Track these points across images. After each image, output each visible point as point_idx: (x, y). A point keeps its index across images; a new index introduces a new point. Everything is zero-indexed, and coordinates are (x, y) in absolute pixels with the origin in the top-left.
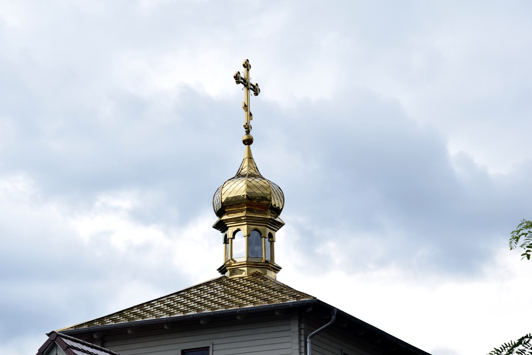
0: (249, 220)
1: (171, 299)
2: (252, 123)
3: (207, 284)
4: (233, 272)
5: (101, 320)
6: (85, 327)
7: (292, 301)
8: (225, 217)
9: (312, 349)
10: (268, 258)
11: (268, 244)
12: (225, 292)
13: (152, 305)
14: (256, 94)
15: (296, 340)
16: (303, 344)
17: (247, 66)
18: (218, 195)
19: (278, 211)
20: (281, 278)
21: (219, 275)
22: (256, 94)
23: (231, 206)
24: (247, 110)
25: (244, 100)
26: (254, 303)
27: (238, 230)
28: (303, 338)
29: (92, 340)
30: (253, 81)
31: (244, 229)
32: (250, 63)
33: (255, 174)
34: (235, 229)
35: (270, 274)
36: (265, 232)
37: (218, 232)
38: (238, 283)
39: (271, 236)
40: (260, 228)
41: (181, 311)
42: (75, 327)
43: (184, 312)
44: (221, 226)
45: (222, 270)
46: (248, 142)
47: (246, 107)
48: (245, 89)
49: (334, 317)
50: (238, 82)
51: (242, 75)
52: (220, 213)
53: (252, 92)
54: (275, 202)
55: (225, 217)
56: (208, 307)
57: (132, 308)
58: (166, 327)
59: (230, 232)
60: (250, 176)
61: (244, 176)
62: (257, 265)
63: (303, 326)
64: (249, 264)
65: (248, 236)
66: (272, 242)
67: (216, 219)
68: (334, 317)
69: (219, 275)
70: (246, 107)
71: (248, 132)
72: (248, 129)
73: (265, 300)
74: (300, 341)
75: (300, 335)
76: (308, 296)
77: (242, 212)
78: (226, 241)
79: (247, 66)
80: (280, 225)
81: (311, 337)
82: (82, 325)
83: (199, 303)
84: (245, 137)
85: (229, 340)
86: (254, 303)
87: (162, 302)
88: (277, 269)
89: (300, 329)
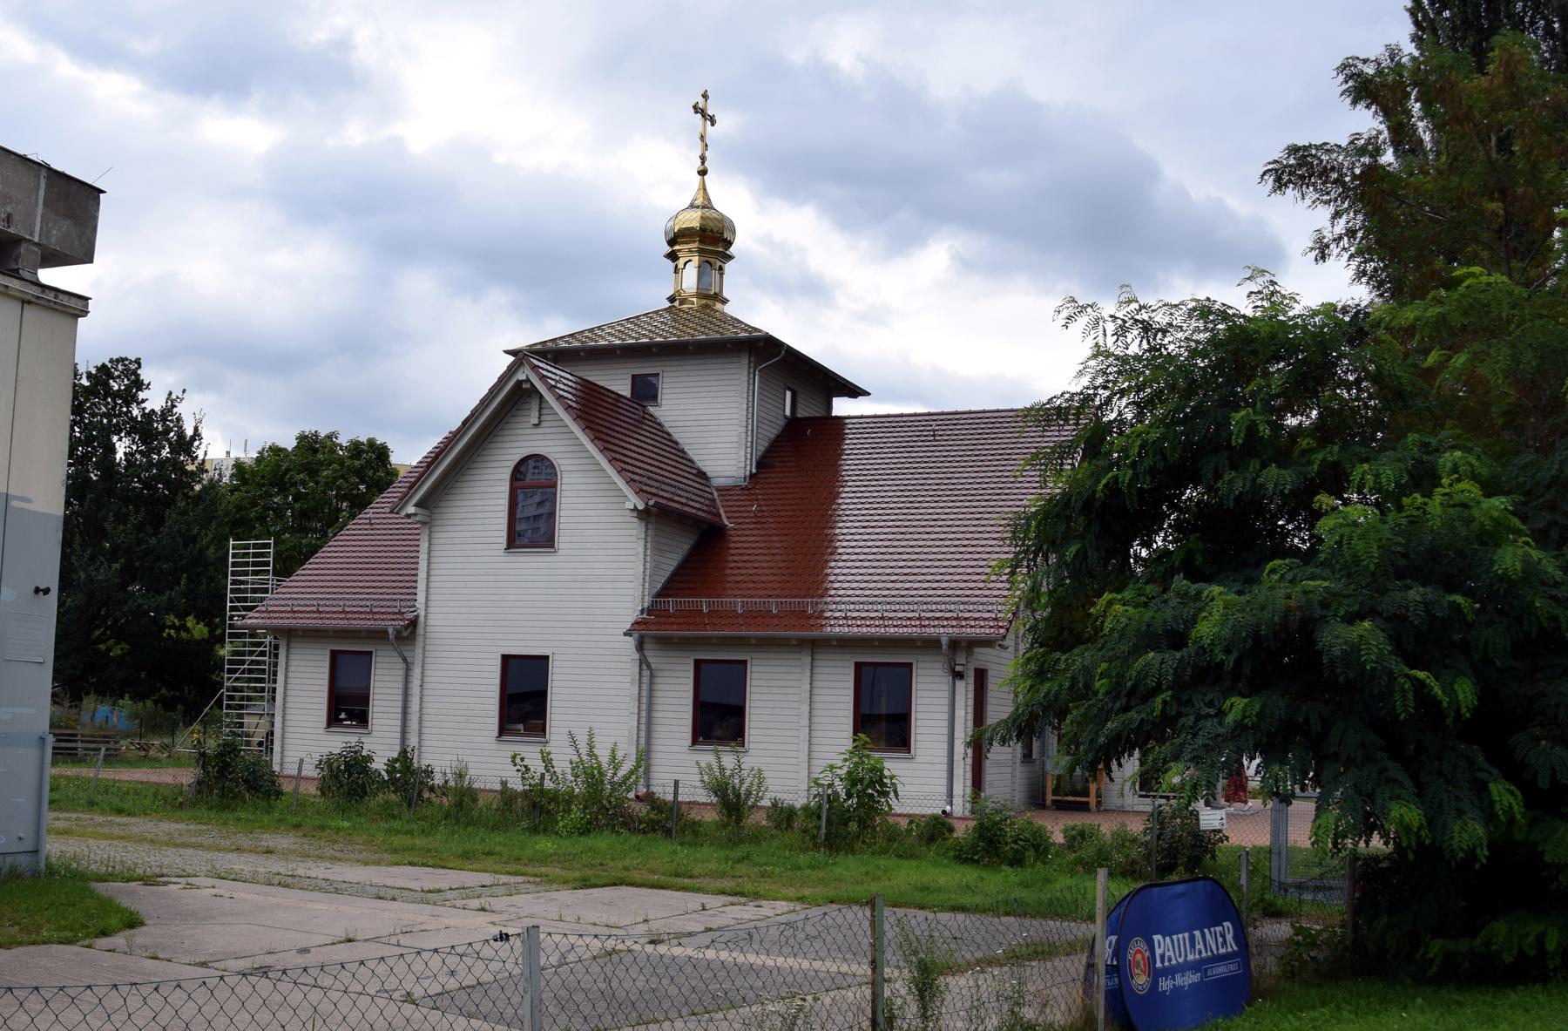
0: (701, 252)
1: (622, 325)
2: (707, 154)
3: (656, 312)
4: (681, 304)
5: (554, 340)
6: (539, 347)
7: (744, 334)
8: (677, 247)
9: (760, 382)
10: (717, 291)
11: (718, 275)
12: (675, 320)
13: (603, 330)
14: (713, 125)
15: (746, 372)
16: (752, 376)
17: (705, 96)
18: (671, 223)
19: (729, 244)
20: (729, 309)
21: (668, 304)
22: (713, 125)
23: (683, 236)
24: (702, 141)
25: (700, 129)
26: (707, 334)
27: (690, 261)
28: (752, 371)
29: (545, 358)
30: (710, 112)
31: (696, 260)
32: (709, 93)
33: (707, 205)
34: (687, 259)
35: (718, 306)
36: (715, 264)
37: (669, 262)
38: (687, 313)
39: (721, 268)
40: (712, 260)
41: (633, 338)
42: (530, 346)
43: (637, 339)
44: (673, 256)
45: (672, 299)
46: (703, 173)
47: (702, 138)
48: (702, 120)
49: (783, 352)
50: (696, 112)
51: (700, 106)
52: (671, 242)
53: (709, 123)
54: (726, 235)
55: (677, 247)
56: (661, 336)
57: (583, 332)
58: (618, 352)
59: (681, 263)
60: (704, 207)
61: (698, 207)
62: (707, 297)
63: (752, 359)
64: (700, 295)
65: (699, 267)
66: (722, 275)
67: (668, 249)
68: (783, 352)
69: (668, 304)
70: (702, 138)
71: (703, 163)
72: (703, 159)
73: (717, 332)
74: (749, 373)
75: (750, 367)
76: (760, 331)
77: (694, 242)
78: (676, 270)
79: (705, 96)
80: (730, 258)
81: (760, 370)
82: (536, 344)
83: (650, 331)
84: (702, 168)
85: (679, 368)
86: (707, 334)
87: (613, 328)
88: (725, 301)
89: (750, 362)
